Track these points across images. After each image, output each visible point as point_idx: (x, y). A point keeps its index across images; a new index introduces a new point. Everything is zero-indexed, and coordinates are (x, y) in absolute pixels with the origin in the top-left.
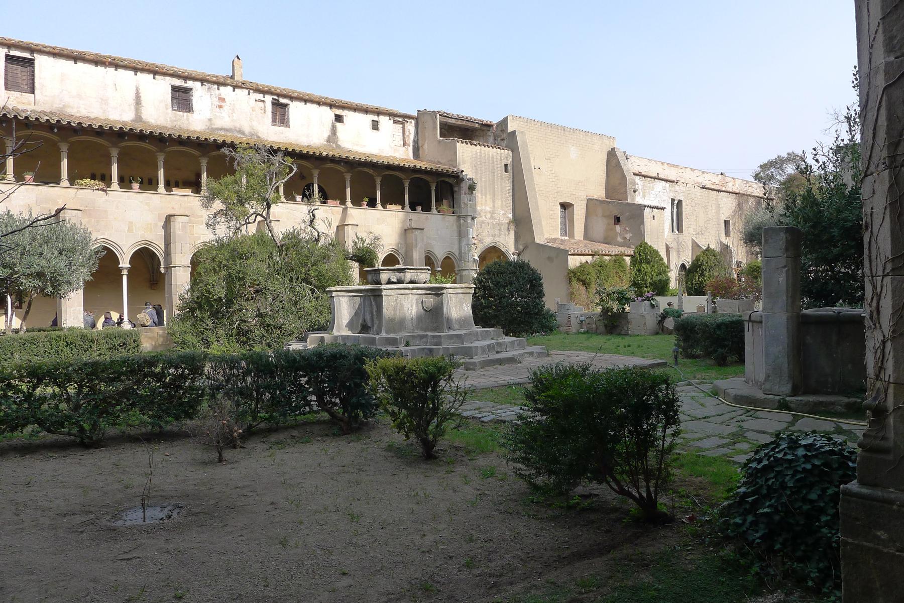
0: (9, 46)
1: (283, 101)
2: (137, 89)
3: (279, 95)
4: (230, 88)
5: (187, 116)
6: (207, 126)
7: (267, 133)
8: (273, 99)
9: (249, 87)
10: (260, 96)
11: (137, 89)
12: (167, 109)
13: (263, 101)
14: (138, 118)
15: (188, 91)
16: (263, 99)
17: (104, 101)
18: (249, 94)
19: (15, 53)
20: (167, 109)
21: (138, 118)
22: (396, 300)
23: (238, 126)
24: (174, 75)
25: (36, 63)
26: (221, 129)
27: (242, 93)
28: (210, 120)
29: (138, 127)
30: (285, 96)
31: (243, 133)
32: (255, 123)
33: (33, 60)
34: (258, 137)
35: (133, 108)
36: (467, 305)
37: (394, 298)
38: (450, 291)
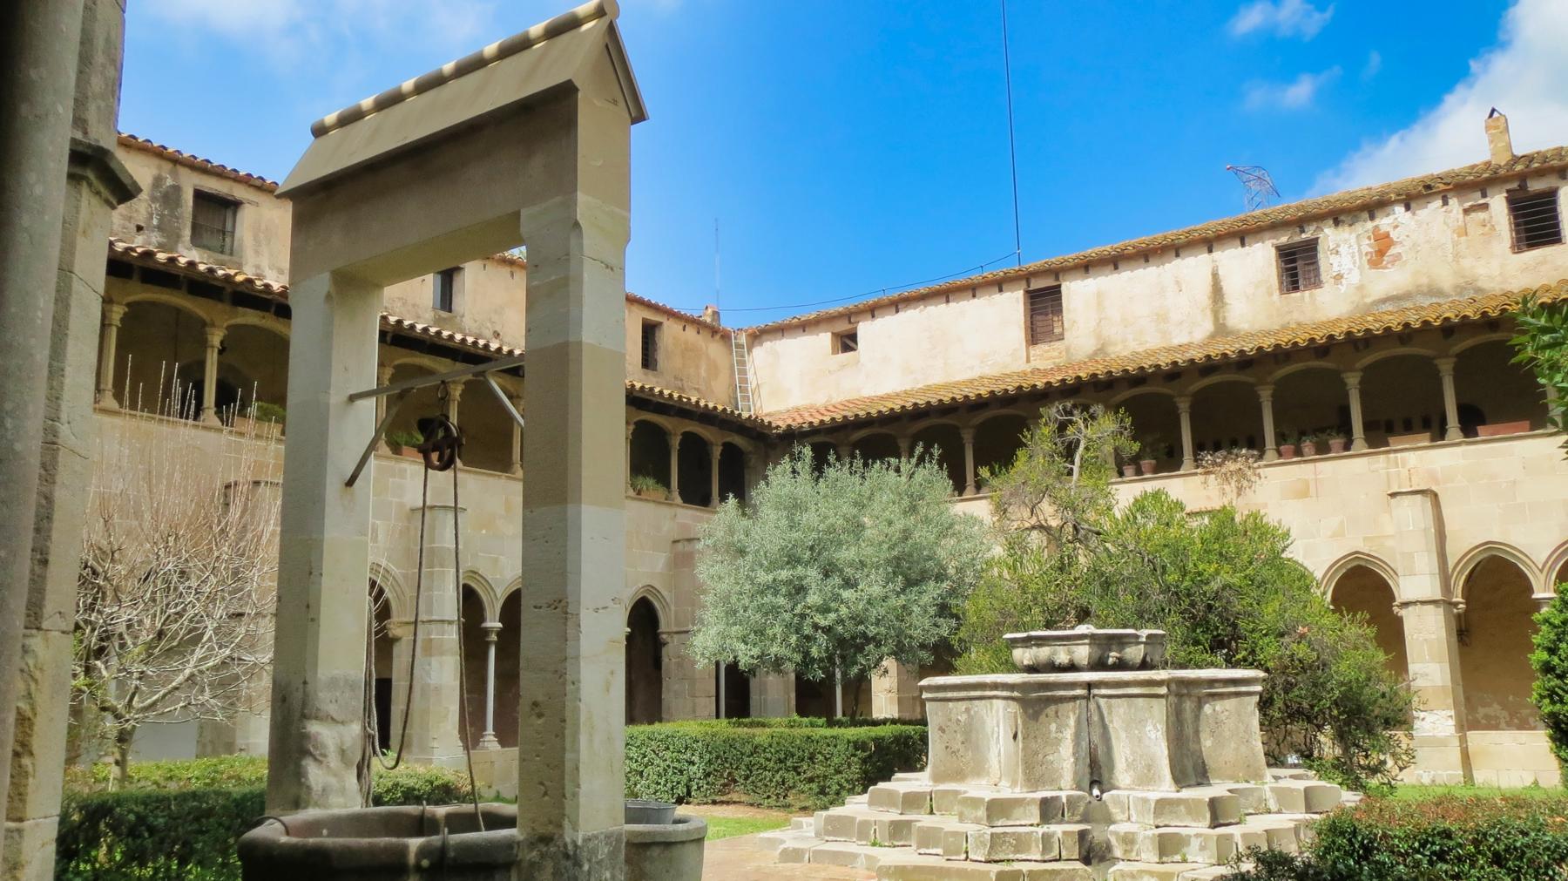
0: (1028, 277)
1: (1536, 186)
2: (1215, 275)
3: (1523, 178)
4: (1399, 209)
5: (1311, 296)
6: (1353, 302)
7: (1501, 274)
8: (1508, 191)
9: (1442, 187)
10: (1476, 198)
11: (1215, 275)
12: (1271, 294)
13: (1485, 207)
14: (1221, 329)
15: (1310, 248)
16: (1482, 201)
17: (1161, 318)
18: (1445, 203)
19: (1037, 284)
20: (1271, 294)
21: (1221, 329)
22: (968, 710)
23: (1424, 280)
24: (1275, 226)
25: (1063, 288)
26: (1384, 301)
27: (1432, 210)
28: (1360, 288)
29: (1230, 348)
30: (1540, 173)
31: (1439, 293)
32: (1466, 263)
33: (1059, 286)
34: (1479, 290)
35: (1209, 313)
36: (1155, 726)
37: (963, 706)
38: (1104, 691)
